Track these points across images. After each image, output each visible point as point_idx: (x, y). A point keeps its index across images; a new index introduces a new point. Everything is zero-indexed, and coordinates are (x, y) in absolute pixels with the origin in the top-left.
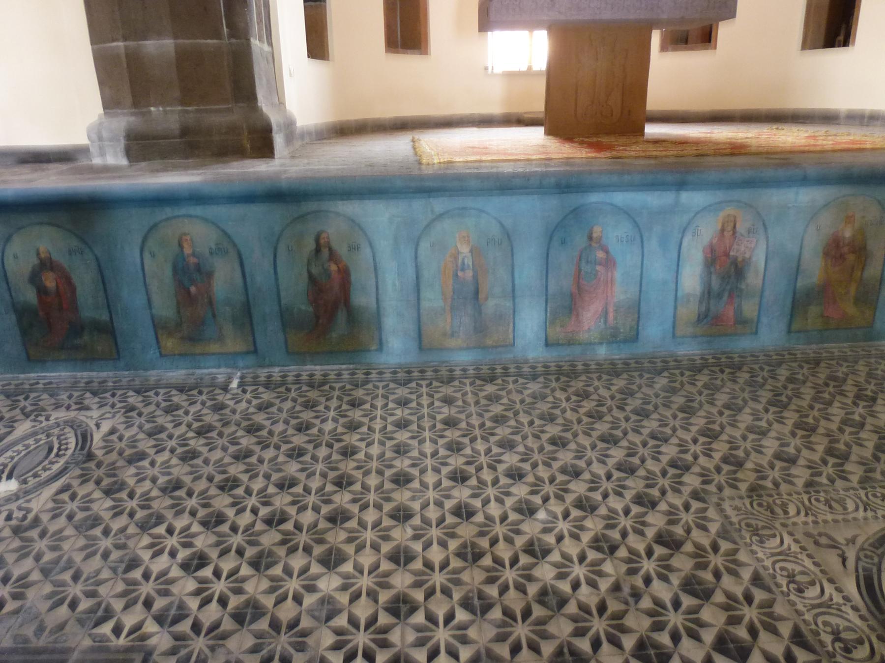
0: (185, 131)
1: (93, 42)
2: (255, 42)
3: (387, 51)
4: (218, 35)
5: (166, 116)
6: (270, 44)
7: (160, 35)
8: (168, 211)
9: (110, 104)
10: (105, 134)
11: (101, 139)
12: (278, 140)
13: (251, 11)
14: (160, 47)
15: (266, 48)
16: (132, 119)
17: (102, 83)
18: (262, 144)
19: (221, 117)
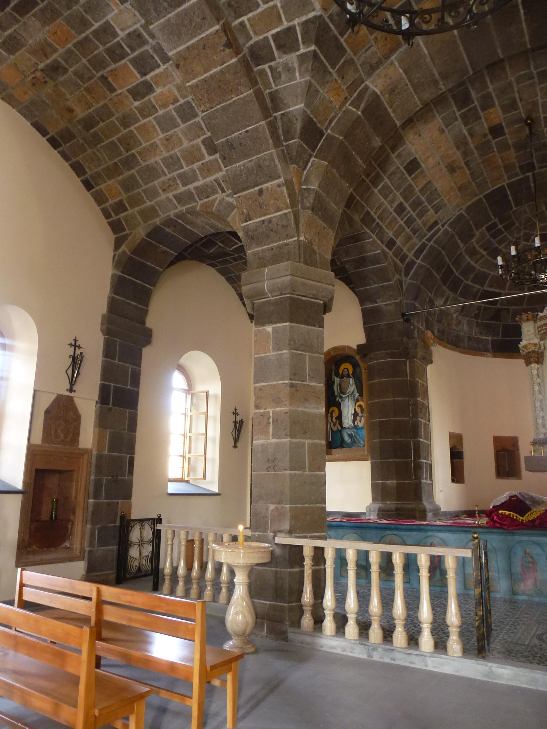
0: (397, 509)
1: (372, 480)
2: (424, 481)
3: (496, 478)
4: (410, 479)
5: (391, 504)
6: (431, 480)
7: (392, 479)
8: (388, 532)
9: (374, 499)
10: (372, 509)
11: (370, 511)
12: (429, 515)
13: (423, 471)
14: (392, 482)
15: (429, 482)
16: (380, 505)
17: (373, 493)
18: (423, 515)
19: (409, 505)
